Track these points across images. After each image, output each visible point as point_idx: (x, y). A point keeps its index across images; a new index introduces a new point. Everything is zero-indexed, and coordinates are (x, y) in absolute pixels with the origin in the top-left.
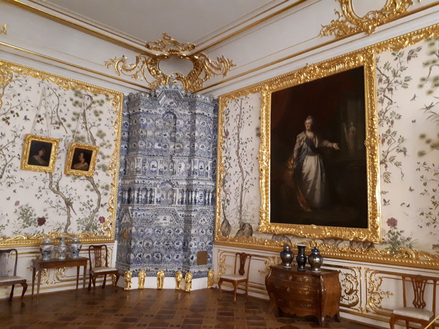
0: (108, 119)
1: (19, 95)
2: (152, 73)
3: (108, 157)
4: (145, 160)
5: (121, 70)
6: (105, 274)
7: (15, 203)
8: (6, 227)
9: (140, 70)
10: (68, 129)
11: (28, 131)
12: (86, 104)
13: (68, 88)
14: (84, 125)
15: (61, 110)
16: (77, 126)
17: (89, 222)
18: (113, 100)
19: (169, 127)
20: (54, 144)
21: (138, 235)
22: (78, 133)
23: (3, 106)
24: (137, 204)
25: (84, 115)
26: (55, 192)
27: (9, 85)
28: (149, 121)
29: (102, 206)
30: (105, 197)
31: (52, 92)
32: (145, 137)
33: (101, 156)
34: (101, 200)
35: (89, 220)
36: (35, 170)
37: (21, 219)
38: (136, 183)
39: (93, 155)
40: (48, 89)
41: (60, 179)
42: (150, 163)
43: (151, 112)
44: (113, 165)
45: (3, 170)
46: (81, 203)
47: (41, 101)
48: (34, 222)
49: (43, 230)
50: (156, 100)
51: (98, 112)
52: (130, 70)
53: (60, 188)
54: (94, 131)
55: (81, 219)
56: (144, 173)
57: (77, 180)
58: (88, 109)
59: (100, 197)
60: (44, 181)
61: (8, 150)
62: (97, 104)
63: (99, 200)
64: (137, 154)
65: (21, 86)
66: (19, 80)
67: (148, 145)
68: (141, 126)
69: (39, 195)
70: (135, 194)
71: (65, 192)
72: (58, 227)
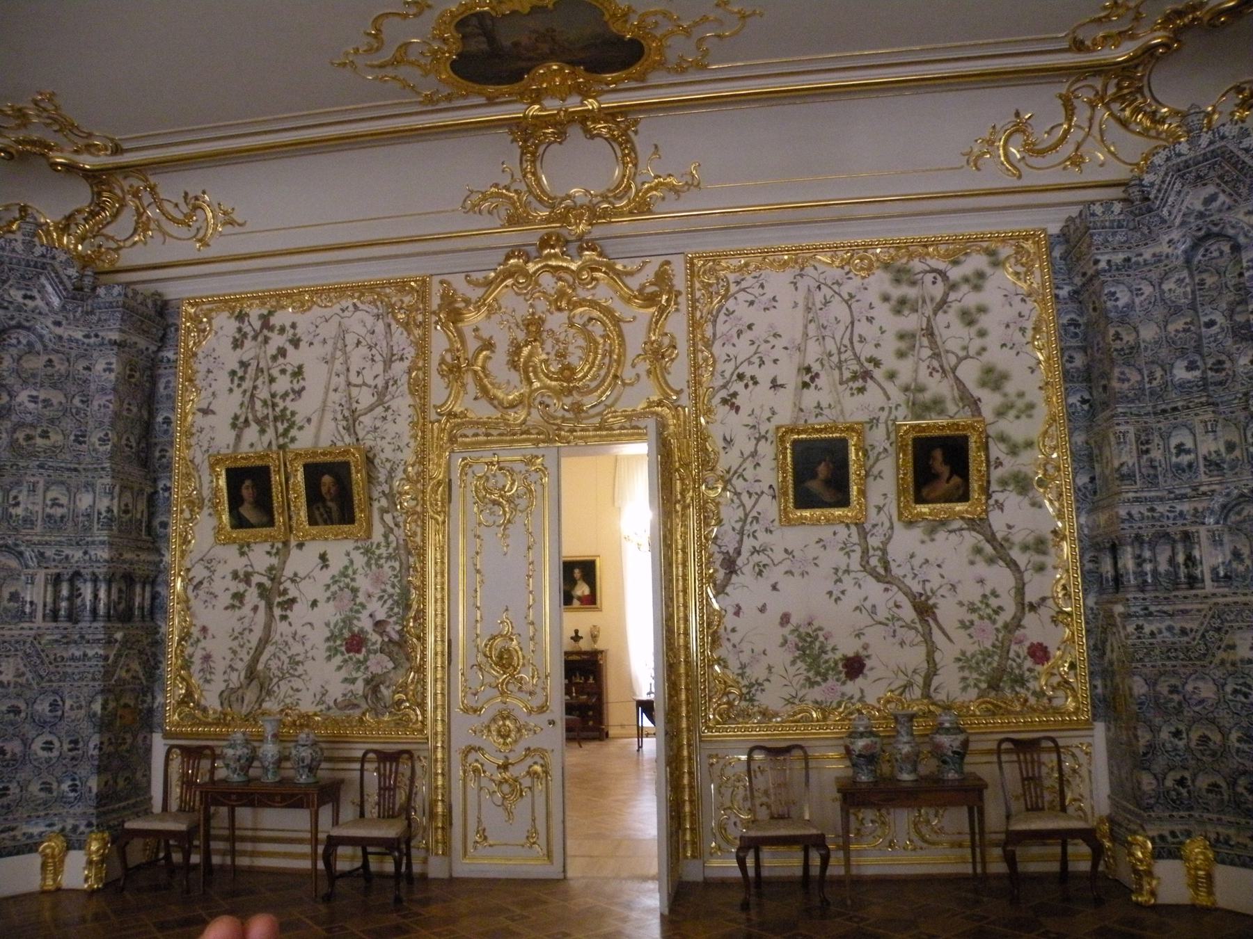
0: (1008, 326)
1: (750, 327)
2: (1132, 126)
3: (1029, 444)
4: (1146, 430)
5: (1023, 158)
6: (1064, 836)
7: (779, 620)
8: (766, 684)
9: (1088, 134)
10: (889, 386)
11: (785, 417)
12: (932, 299)
13: (870, 269)
14: (935, 364)
15: (860, 336)
16: (916, 371)
17: (995, 665)
18: (1012, 260)
19: (1221, 288)
20: (853, 441)
21: (1159, 704)
22: (921, 389)
23: (720, 367)
24: (1141, 595)
25: (930, 332)
26: (878, 578)
27: (724, 310)
28: (1139, 292)
29: (1033, 608)
30: (1037, 577)
31: (829, 293)
32: (1134, 349)
33: (1003, 447)
34: (1027, 589)
35: (996, 658)
36: (816, 522)
37: (799, 664)
38: (1123, 521)
39: (972, 445)
40: (819, 287)
41: (890, 538)
42: (1165, 437)
43: (1141, 259)
44: (1051, 471)
45: (741, 533)
46: (961, 604)
47: (806, 327)
48: (833, 669)
49: (862, 691)
50: (1150, 210)
51: (973, 310)
52: (1054, 147)
53: (893, 566)
54: (969, 373)
55: (968, 654)
56: (1152, 481)
57: (941, 535)
58: (940, 313)
59: (1022, 579)
60: (846, 549)
61: (745, 480)
62: (965, 288)
63: (1020, 591)
64: (1113, 416)
65: (752, 303)
66: (744, 290)
67: (1152, 378)
68: (1112, 315)
69: (836, 593)
70: (1128, 561)
71: (910, 576)
72: (903, 683)
